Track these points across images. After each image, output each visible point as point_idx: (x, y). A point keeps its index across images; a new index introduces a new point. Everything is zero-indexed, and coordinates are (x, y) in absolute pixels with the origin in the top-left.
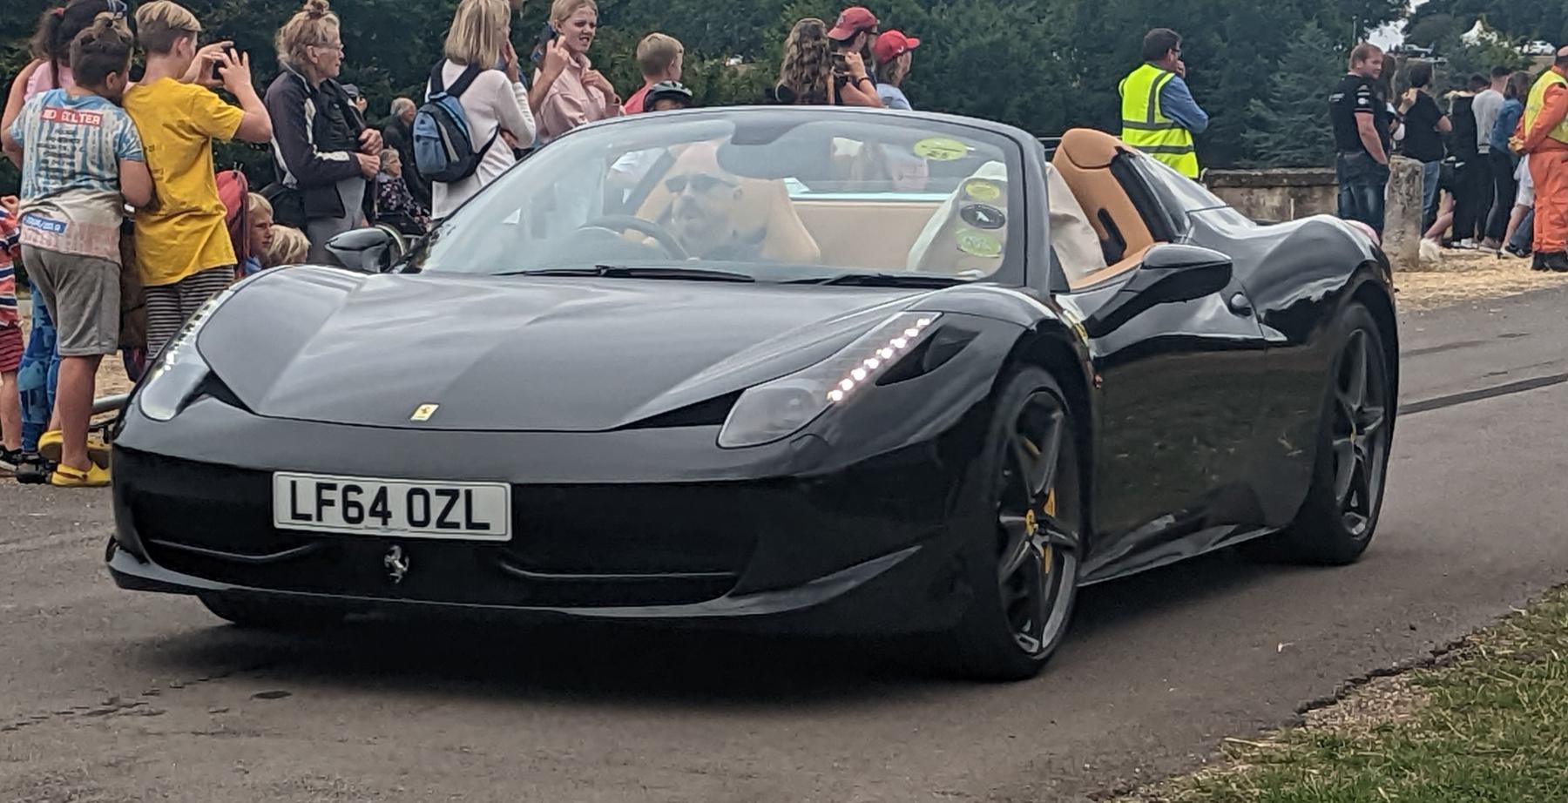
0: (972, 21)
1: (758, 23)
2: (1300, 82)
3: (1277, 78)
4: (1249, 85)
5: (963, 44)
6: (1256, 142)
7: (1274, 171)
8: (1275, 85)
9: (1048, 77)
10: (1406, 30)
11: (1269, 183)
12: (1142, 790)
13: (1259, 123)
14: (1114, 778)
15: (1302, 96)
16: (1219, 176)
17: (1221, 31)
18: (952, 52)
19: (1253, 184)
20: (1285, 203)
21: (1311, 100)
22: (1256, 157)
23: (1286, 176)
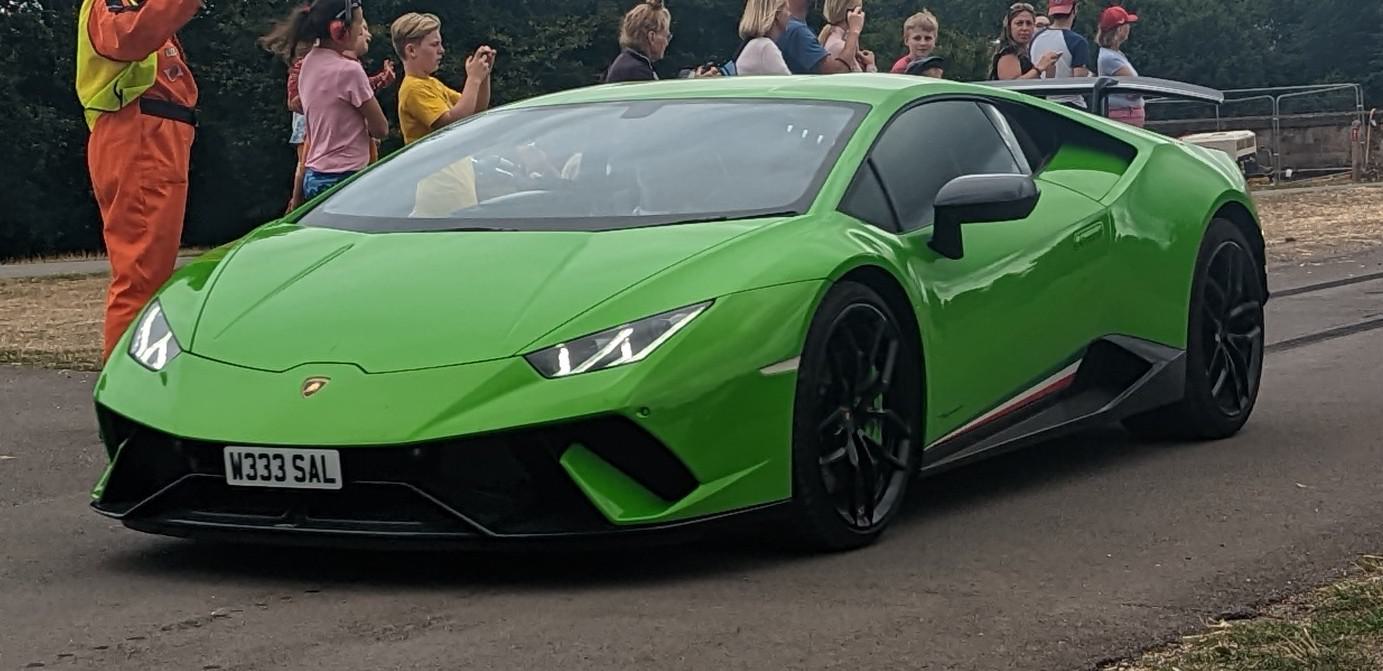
9: (1251, 43)
12: (1292, 599)
14: (1269, 590)
18: (1173, 27)
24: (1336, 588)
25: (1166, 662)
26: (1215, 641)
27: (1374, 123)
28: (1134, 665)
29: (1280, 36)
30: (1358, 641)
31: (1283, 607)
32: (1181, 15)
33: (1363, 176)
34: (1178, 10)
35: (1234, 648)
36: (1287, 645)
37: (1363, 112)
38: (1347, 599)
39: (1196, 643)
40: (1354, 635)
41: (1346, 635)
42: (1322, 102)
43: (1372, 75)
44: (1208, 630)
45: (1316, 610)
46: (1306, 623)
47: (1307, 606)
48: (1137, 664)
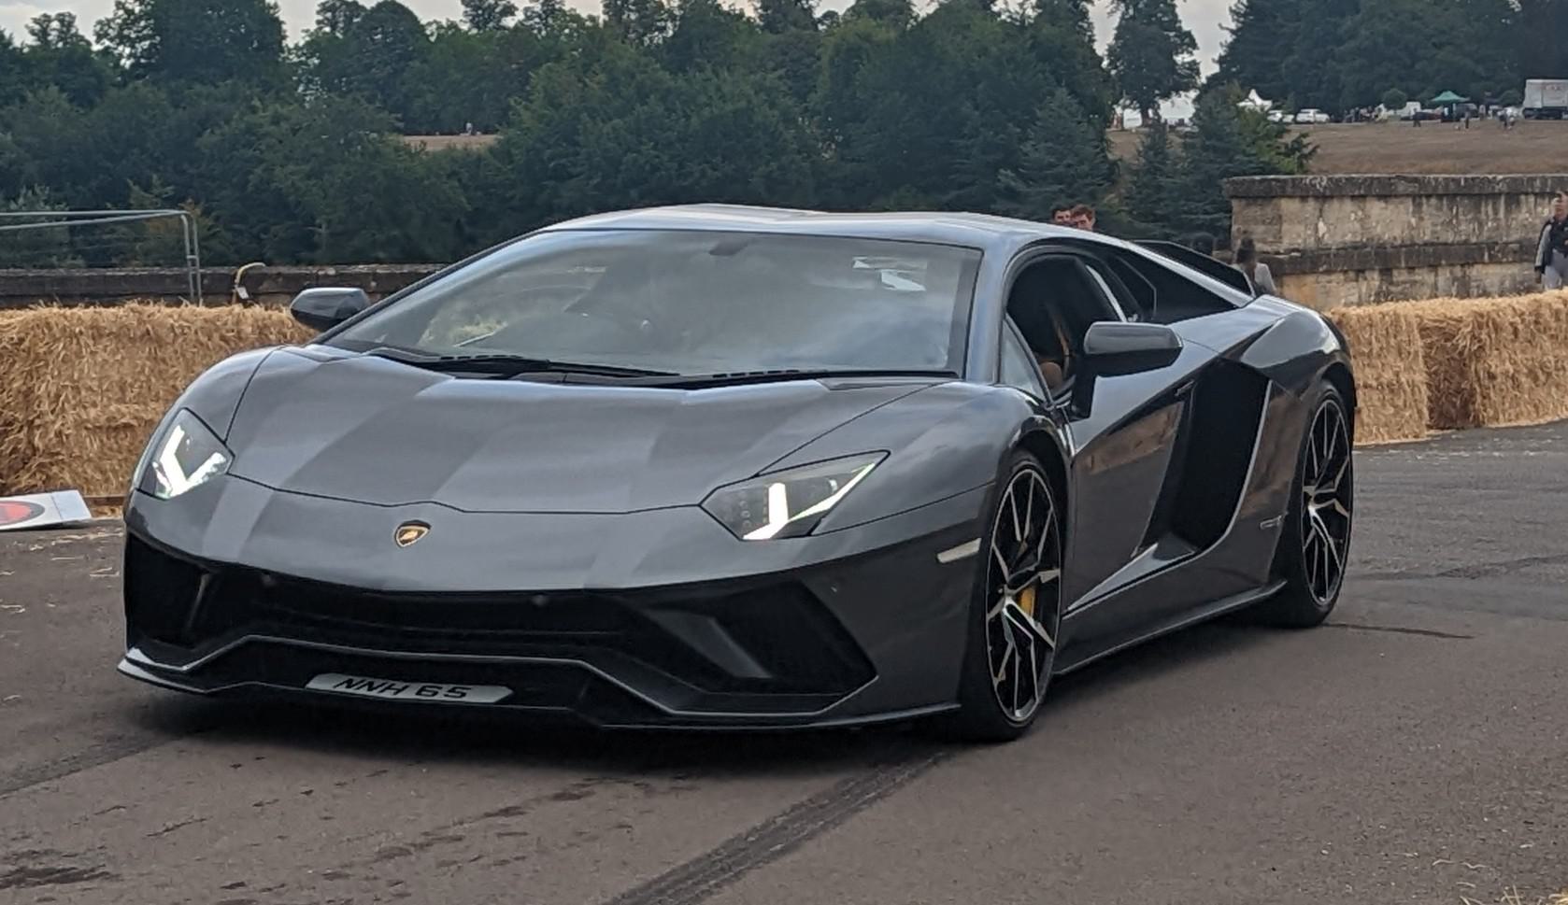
2: (1050, 152)
3: (1027, 147)
10: (1196, 100)
15: (1051, 166)
21: (1061, 169)
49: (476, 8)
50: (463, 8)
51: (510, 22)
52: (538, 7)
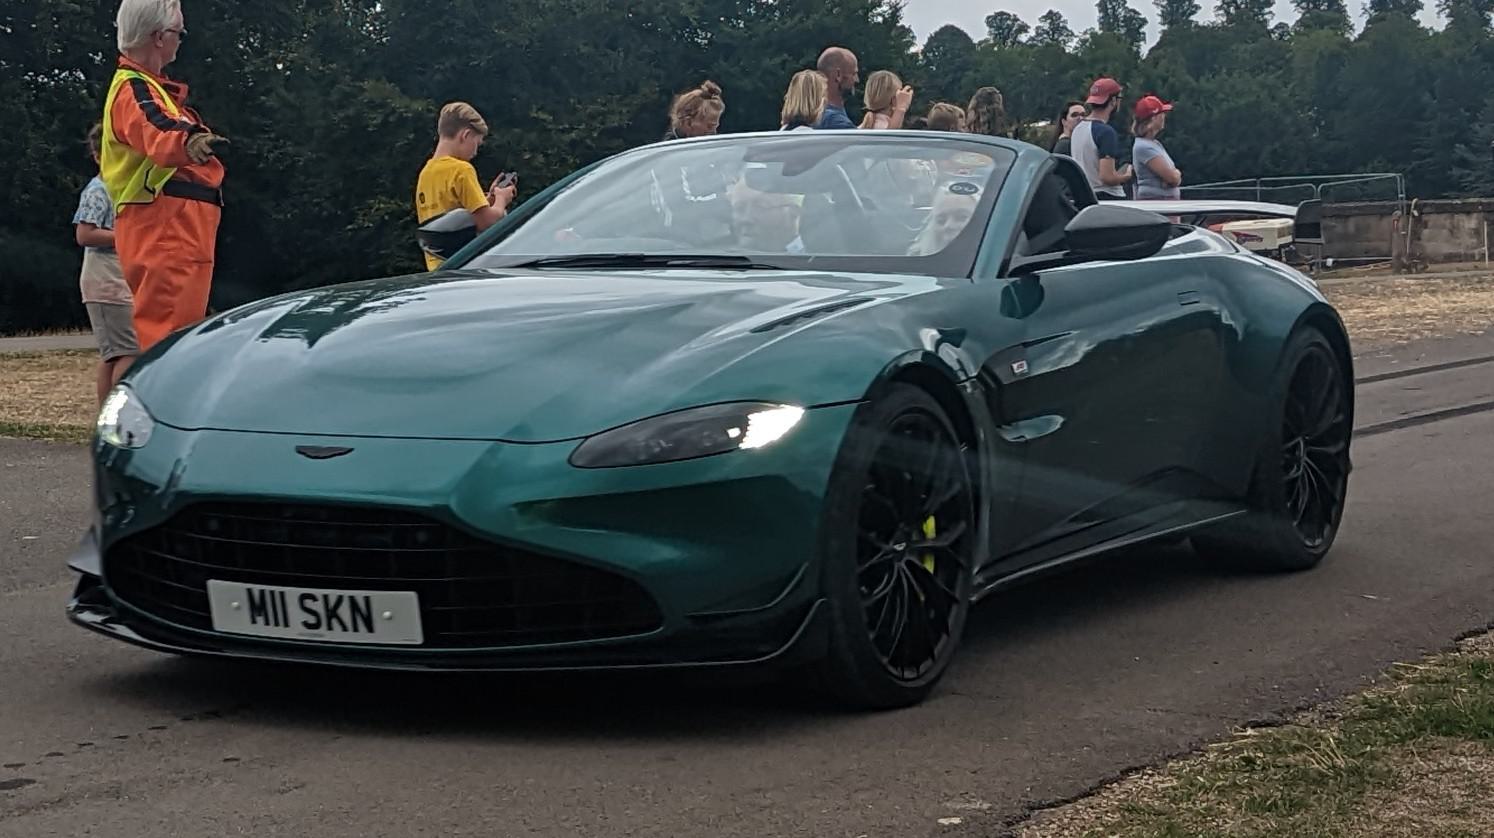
0: (1233, 87)
1: (1061, 93)
3: (1476, 126)
4: (1452, 134)
5: (1225, 106)
6: (1461, 177)
7: (1471, 200)
8: (1476, 133)
9: (1293, 129)
11: (1468, 209)
13: (1463, 163)
16: (1425, 205)
17: (1432, 92)
18: (1216, 113)
19: (1453, 210)
20: (1480, 224)
22: (1461, 189)
23: (1481, 204)
24: (1364, 697)
25: (1190, 771)
26: (1239, 750)
27: (1416, 213)
28: (1159, 774)
29: (1323, 123)
30: (1384, 753)
31: (1310, 716)
32: (1223, 100)
33: (1404, 266)
34: (1221, 96)
35: (1259, 757)
36: (1313, 756)
37: (1405, 202)
38: (1375, 708)
39: (1222, 751)
40: (1380, 746)
41: (1372, 746)
42: (1365, 192)
43: (1414, 163)
44: (1234, 738)
45: (1344, 719)
46: (1332, 734)
47: (1334, 714)
48: (1162, 772)
49: (999, 28)
50: (987, 29)
51: (1023, 38)
52: (1046, 26)
